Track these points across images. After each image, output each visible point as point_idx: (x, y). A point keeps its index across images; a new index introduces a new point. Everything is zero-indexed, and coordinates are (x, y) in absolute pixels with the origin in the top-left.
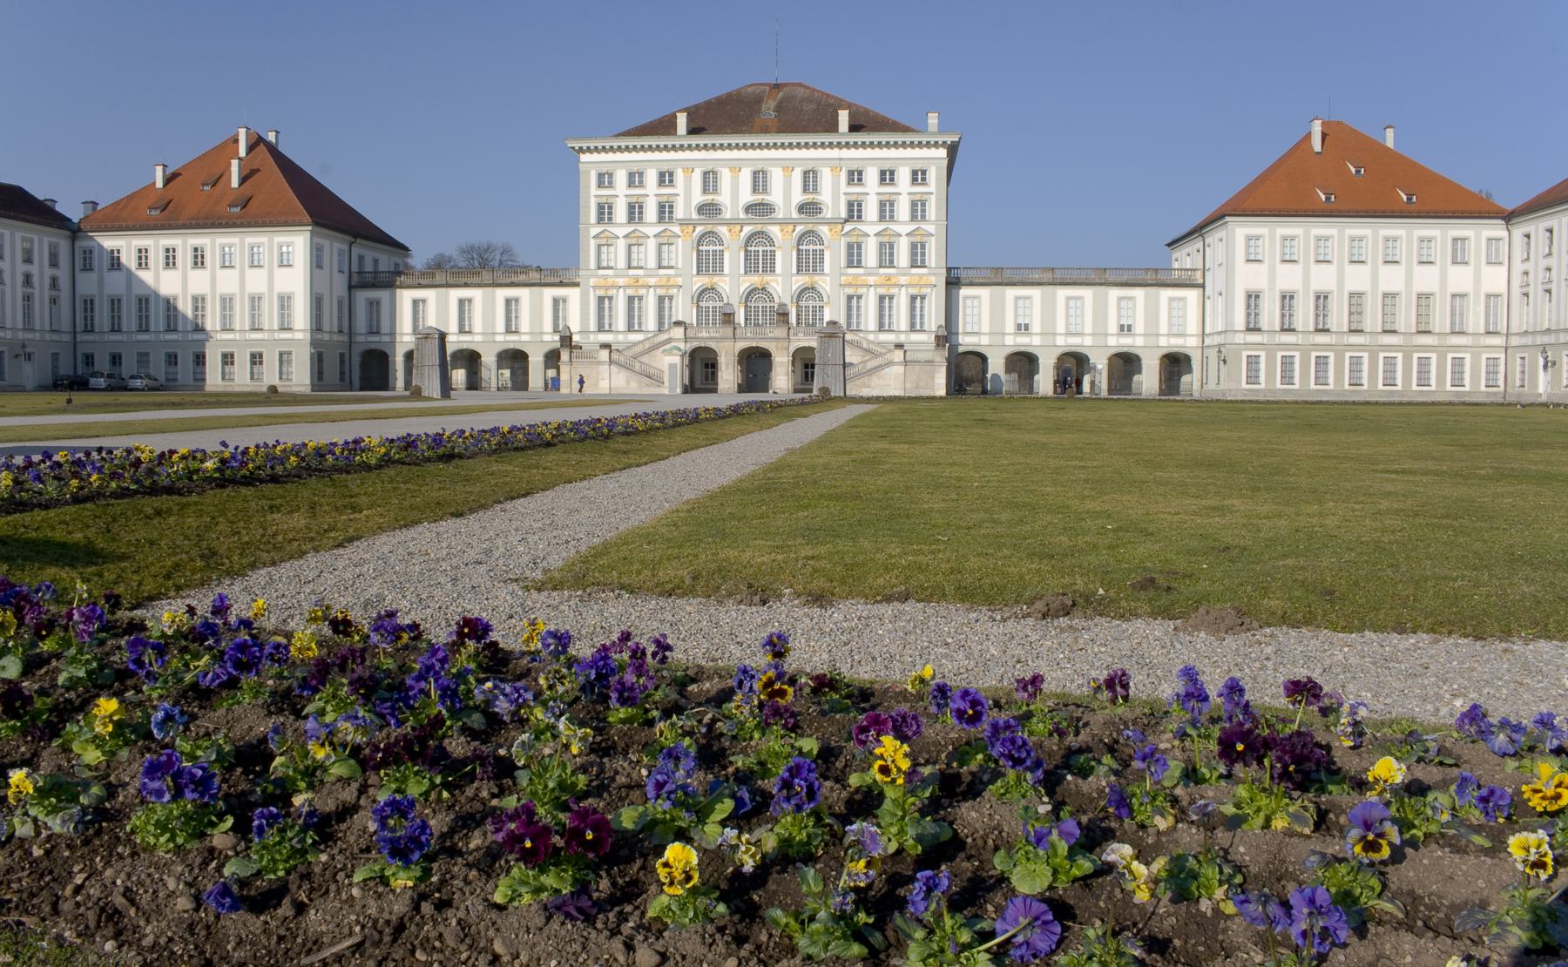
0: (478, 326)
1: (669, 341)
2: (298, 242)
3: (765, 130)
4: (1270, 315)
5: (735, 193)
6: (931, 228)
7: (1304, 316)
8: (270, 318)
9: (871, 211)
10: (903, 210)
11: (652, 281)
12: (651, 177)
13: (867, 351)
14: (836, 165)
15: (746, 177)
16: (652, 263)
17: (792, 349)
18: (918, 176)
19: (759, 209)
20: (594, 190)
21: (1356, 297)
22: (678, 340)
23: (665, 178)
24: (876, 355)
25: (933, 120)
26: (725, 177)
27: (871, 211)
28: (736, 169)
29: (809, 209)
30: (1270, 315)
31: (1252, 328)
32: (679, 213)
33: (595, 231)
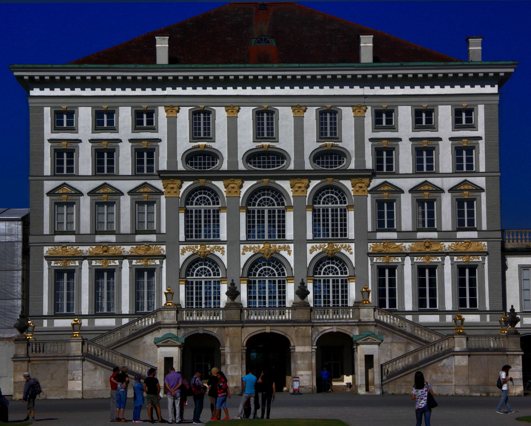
1: (157, 326)
6: (481, 182)
9: (405, 160)
10: (445, 159)
11: (127, 249)
13: (412, 338)
14: (358, 104)
17: (316, 337)
18: (463, 116)
19: (266, 159)
20: (48, 133)
22: (169, 326)
23: (144, 118)
24: (427, 344)
25: (475, 47)
27: (405, 160)
28: (233, 105)
29: (329, 157)
33: (49, 185)
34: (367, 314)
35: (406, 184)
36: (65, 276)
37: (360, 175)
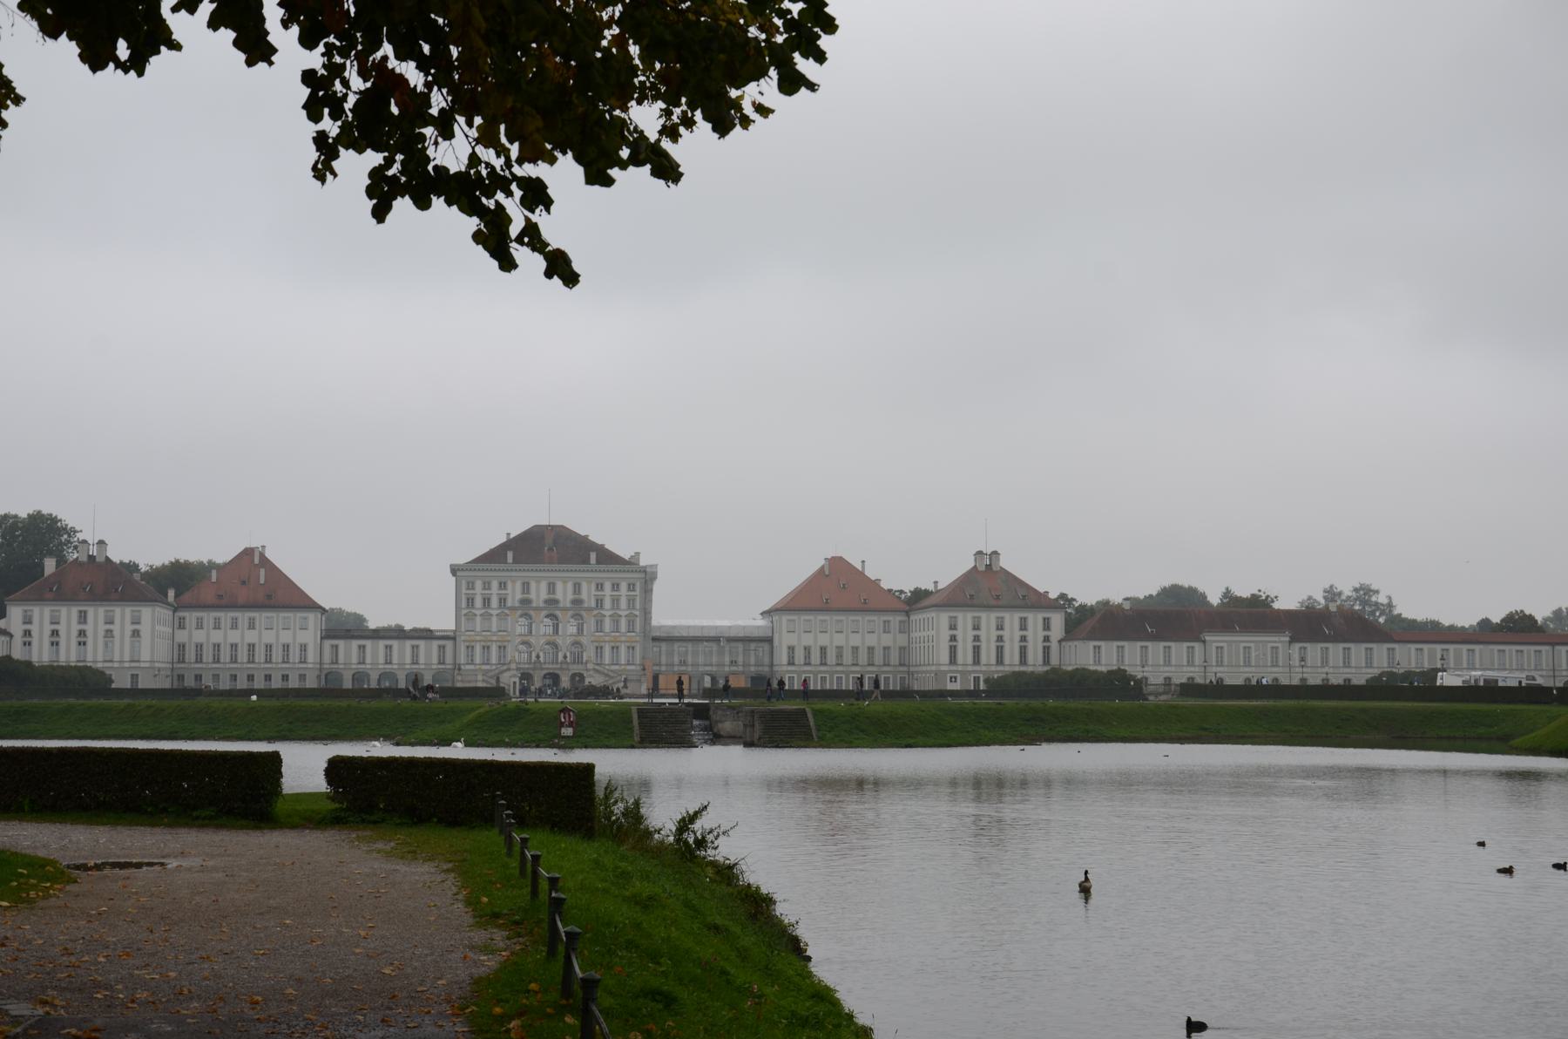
0: (395, 660)
2: (312, 618)
3: (551, 562)
4: (800, 657)
5: (539, 593)
7: (815, 657)
8: (295, 655)
10: (623, 603)
12: (495, 584)
15: (544, 585)
16: (494, 629)
18: (631, 587)
19: (551, 602)
21: (840, 648)
23: (503, 585)
26: (533, 585)
27: (607, 604)
29: (577, 602)
30: (800, 657)
31: (791, 663)
32: (509, 604)
34: (590, 666)
35: (608, 613)
36: (470, 648)
37: (589, 609)
